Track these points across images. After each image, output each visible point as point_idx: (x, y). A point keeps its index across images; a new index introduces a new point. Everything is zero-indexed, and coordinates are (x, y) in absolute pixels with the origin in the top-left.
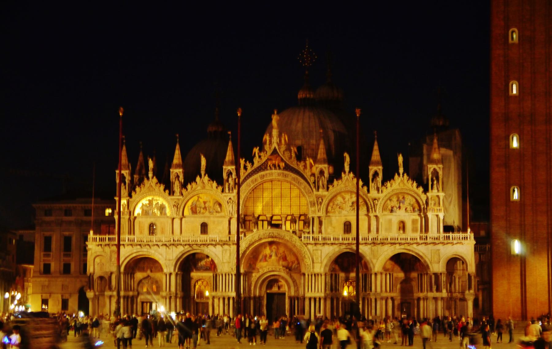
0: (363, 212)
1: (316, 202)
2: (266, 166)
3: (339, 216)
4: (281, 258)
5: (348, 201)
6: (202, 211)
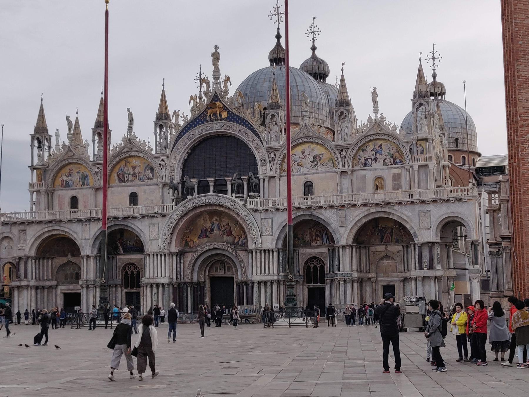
0: (327, 168)
1: (267, 158)
2: (205, 117)
3: (297, 175)
4: (225, 231)
5: (309, 154)
6: (131, 178)
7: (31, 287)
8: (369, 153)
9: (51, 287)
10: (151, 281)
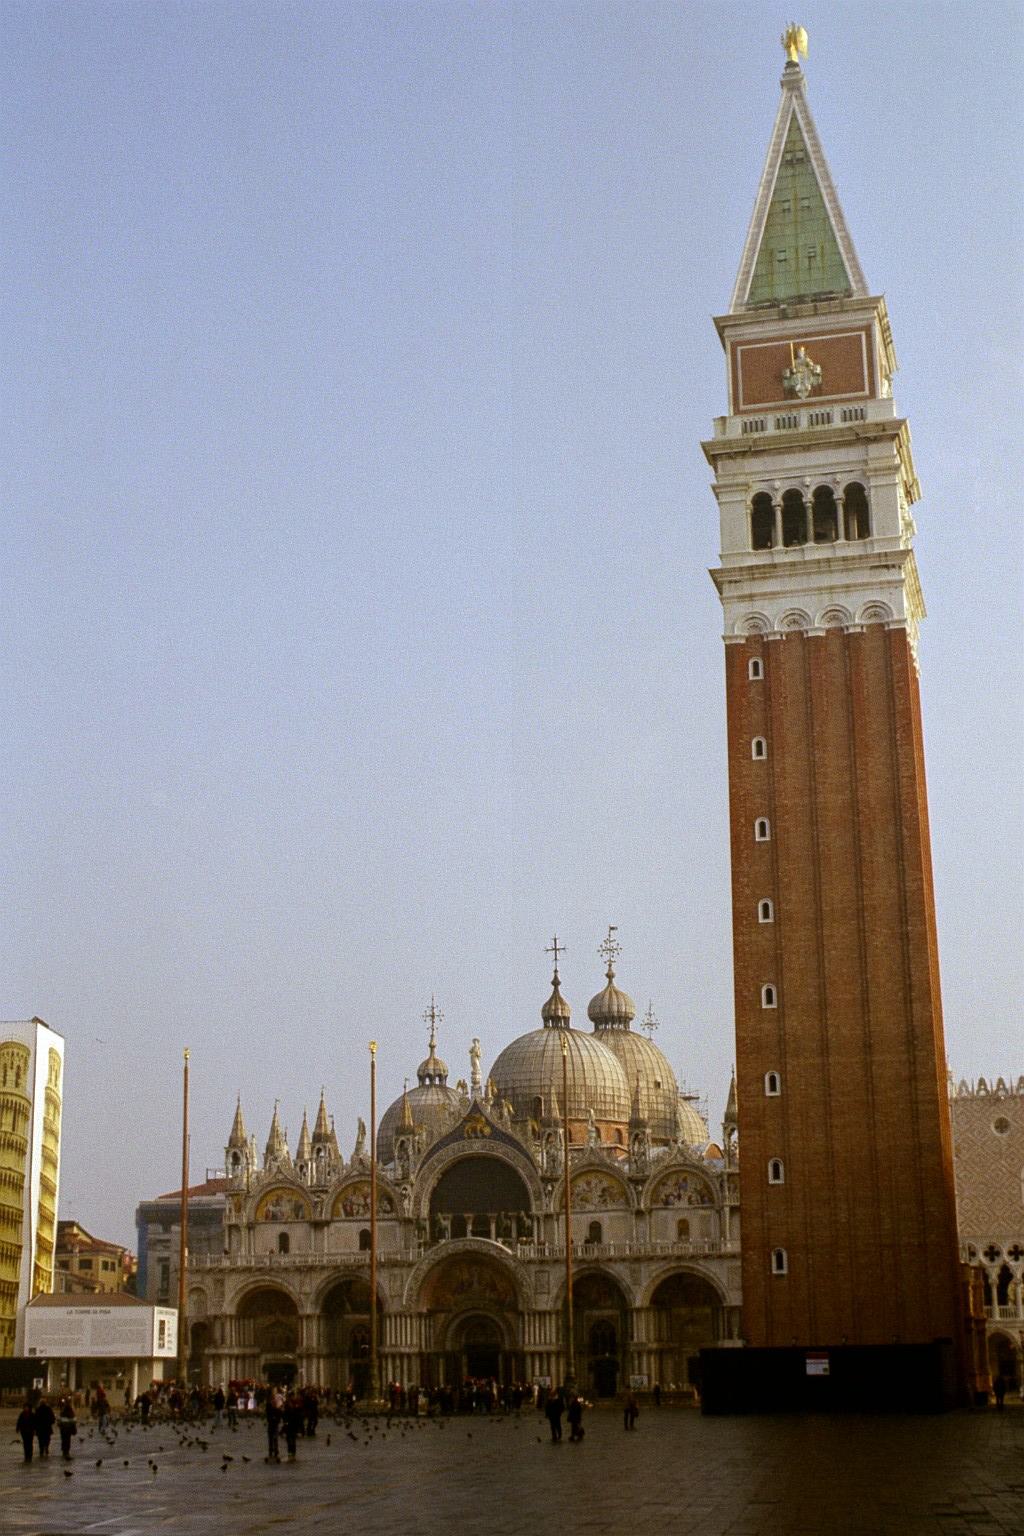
1: (542, 1190)
7: (231, 1356)
8: (670, 1189)
9: (255, 1356)
10: (393, 1350)
